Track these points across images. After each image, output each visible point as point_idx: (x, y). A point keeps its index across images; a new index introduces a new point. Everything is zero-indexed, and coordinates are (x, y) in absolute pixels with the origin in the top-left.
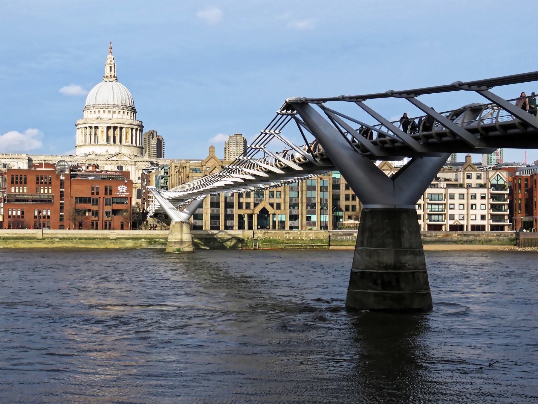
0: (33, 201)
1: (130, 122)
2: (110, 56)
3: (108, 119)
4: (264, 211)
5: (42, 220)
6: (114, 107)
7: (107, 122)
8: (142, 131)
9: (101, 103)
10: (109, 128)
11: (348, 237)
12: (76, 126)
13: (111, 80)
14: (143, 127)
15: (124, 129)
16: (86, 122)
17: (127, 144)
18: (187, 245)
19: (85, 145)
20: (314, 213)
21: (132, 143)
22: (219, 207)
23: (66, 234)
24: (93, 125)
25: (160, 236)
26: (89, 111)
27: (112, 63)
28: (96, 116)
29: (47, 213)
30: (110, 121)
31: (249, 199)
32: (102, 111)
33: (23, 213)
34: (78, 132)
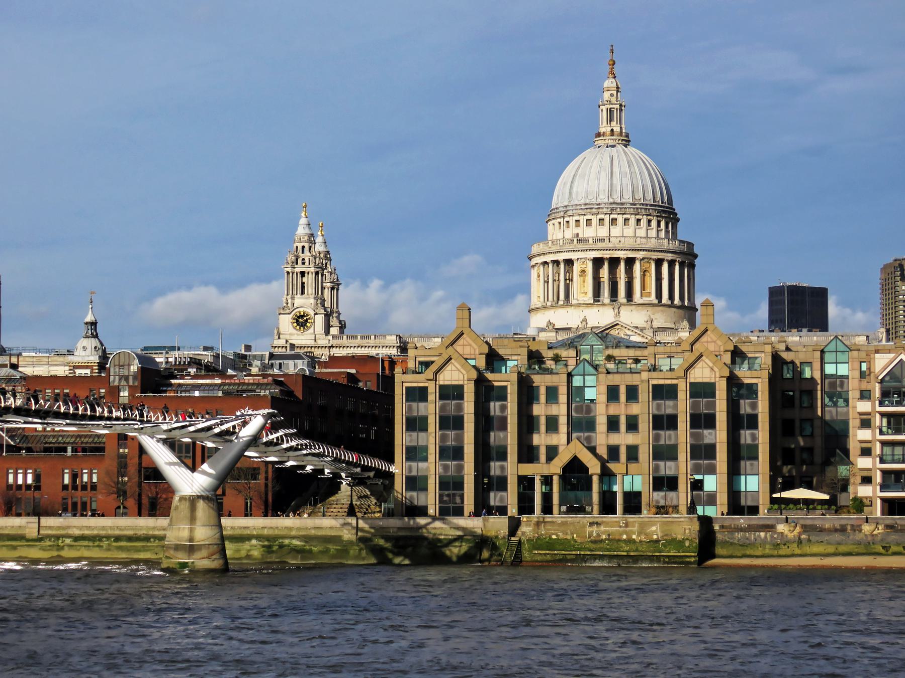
0: (47, 450)
1: (652, 244)
2: (609, 83)
3: (598, 240)
4: (575, 467)
5: (79, 493)
6: (612, 210)
7: (594, 247)
8: (692, 266)
9: (582, 202)
10: (598, 263)
11: (762, 534)
12: (530, 259)
13: (611, 142)
14: (696, 256)
15: (637, 267)
16: (547, 250)
17: (646, 300)
18: (204, 553)
19: (545, 307)
20: (712, 470)
21: (659, 295)
22: (462, 459)
23: (88, 528)
24: (561, 257)
25: (294, 533)
26: (556, 222)
27: (613, 100)
28: (569, 234)
29: (90, 477)
30: (600, 245)
31: (554, 436)
32: (583, 220)
33: (37, 477)
34: (534, 273)
